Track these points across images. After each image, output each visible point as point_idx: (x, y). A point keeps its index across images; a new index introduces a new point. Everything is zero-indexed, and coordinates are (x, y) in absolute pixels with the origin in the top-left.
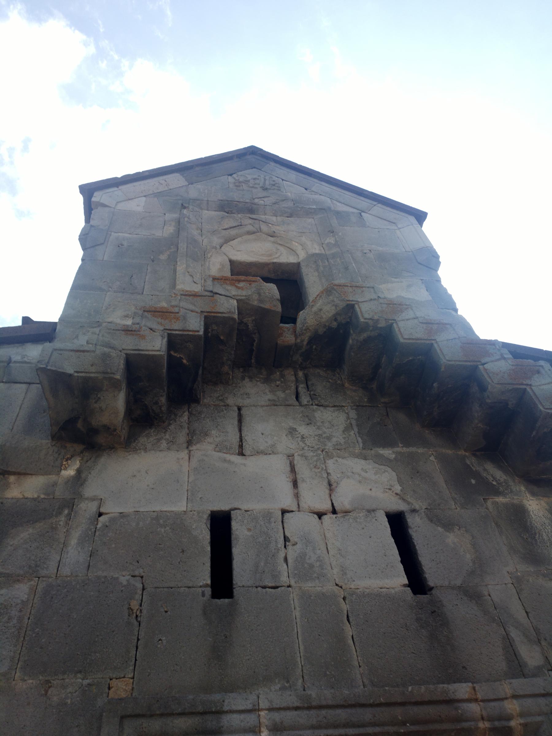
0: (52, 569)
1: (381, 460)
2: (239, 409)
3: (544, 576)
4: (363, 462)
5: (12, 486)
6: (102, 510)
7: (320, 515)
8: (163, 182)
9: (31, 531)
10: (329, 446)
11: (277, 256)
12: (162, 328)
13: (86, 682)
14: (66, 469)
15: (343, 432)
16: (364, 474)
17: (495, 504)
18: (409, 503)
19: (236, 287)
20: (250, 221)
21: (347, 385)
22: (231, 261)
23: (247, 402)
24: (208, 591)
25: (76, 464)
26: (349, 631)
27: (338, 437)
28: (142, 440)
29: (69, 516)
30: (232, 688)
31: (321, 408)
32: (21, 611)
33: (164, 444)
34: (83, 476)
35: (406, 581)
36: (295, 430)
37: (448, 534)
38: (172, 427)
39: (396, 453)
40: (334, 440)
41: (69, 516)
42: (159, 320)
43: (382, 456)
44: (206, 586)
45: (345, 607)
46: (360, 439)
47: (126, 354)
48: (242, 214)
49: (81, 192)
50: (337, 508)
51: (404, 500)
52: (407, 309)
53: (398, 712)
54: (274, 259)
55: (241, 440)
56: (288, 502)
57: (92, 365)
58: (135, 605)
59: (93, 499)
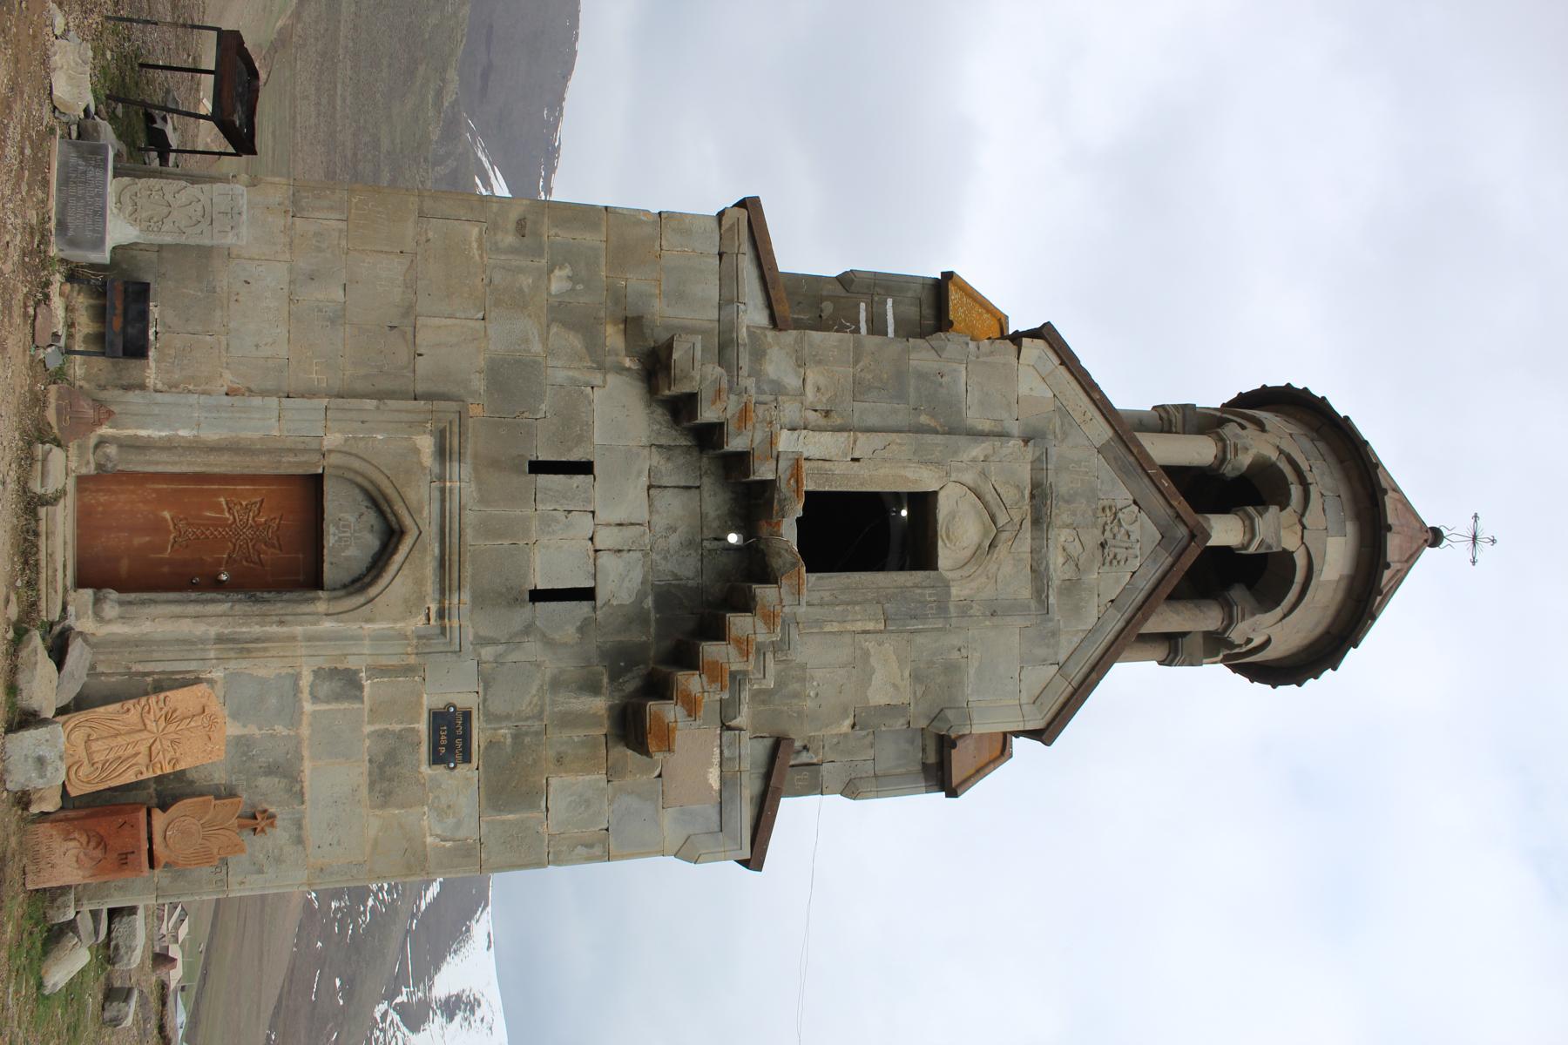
0: (550, 363)
1: (641, 596)
2: (698, 487)
3: (542, 686)
4: (640, 581)
5: (616, 328)
6: (595, 389)
7: (592, 539)
8: (1089, 415)
9: (579, 346)
10: (654, 556)
11: (948, 545)
12: (728, 417)
13: (482, 391)
14: (631, 360)
15: (672, 572)
16: (627, 579)
17: (603, 675)
18: (602, 608)
19: (790, 479)
20: (1017, 520)
21: (728, 584)
22: (935, 493)
23: (706, 495)
24: (534, 459)
25: (634, 367)
26: (506, 542)
27: (665, 566)
28: (659, 411)
29: (592, 368)
30: (476, 470)
31: (699, 557)
32: (524, 350)
33: (656, 427)
34: (625, 373)
35: (538, 588)
36: (675, 531)
37: (575, 628)
38: (674, 432)
39: (649, 613)
40: (664, 562)
41: (592, 368)
42: (738, 415)
43: (645, 595)
44: (537, 457)
45: (522, 543)
46: (663, 583)
47: (697, 393)
48: (1029, 511)
49: (1045, 324)
50: (598, 553)
51: (604, 605)
52: (769, 628)
53: (455, 558)
54: (943, 540)
55: (665, 487)
56: (602, 516)
57: (681, 370)
58: (526, 415)
59: (605, 381)
